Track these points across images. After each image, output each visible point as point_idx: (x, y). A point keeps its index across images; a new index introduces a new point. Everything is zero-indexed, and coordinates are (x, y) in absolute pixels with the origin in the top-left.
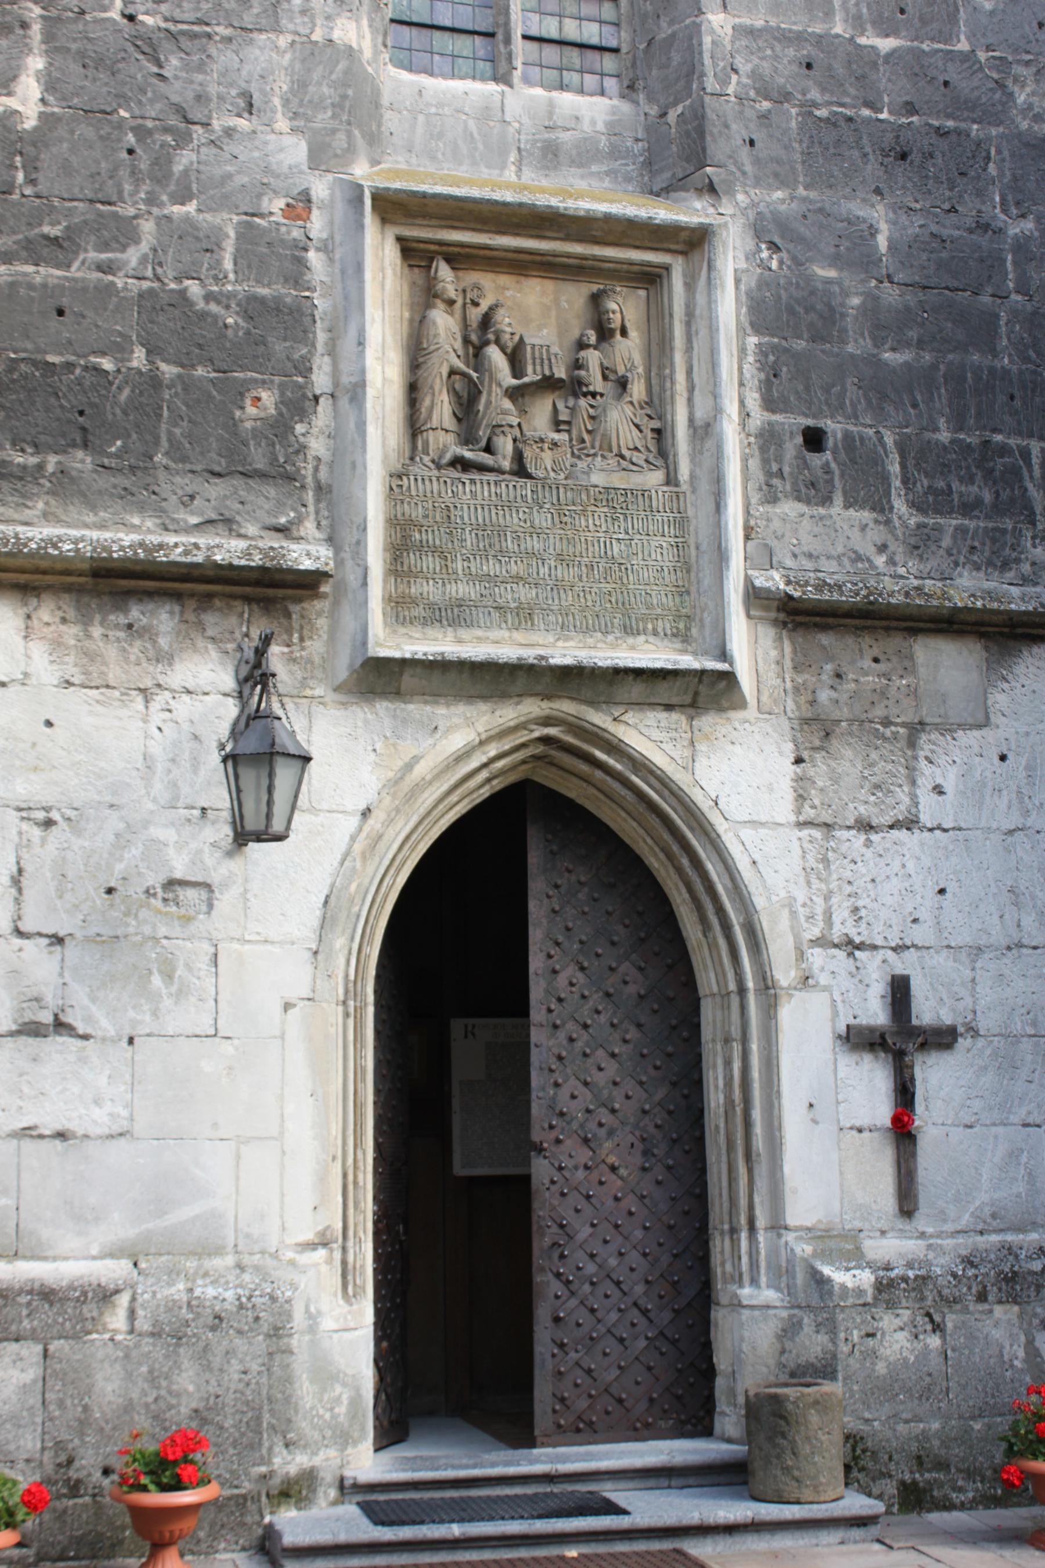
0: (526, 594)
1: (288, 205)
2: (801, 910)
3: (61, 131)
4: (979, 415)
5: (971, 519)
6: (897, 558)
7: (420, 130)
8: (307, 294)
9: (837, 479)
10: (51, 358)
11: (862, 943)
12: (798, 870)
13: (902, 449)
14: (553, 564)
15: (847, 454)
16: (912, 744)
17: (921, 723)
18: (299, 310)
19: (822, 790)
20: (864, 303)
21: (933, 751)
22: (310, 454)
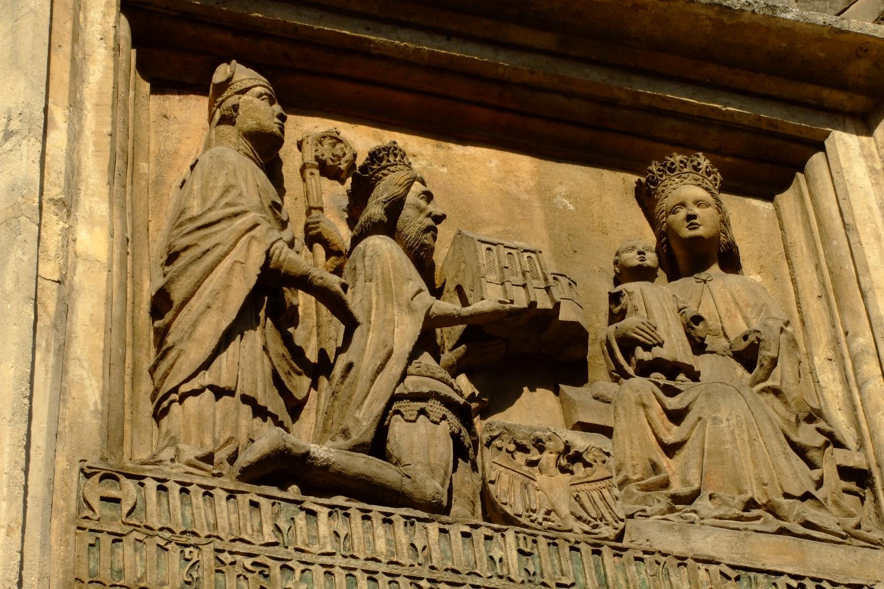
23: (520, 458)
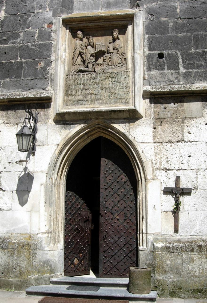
0: (93, 97)
1: (48, 25)
2: (154, 162)
3: (8, 19)
4: (202, 45)
5: (199, 69)
6: (180, 80)
7: (81, 5)
8: (51, 41)
9: (166, 65)
10: (3, 62)
11: (169, 169)
12: (153, 153)
13: (182, 55)
14: (99, 90)
15: (168, 58)
16: (183, 122)
17: (185, 118)
18: (49, 45)
19: (160, 134)
20: (174, 24)
21: (188, 124)
22: (50, 73)
23: (97, 66)
